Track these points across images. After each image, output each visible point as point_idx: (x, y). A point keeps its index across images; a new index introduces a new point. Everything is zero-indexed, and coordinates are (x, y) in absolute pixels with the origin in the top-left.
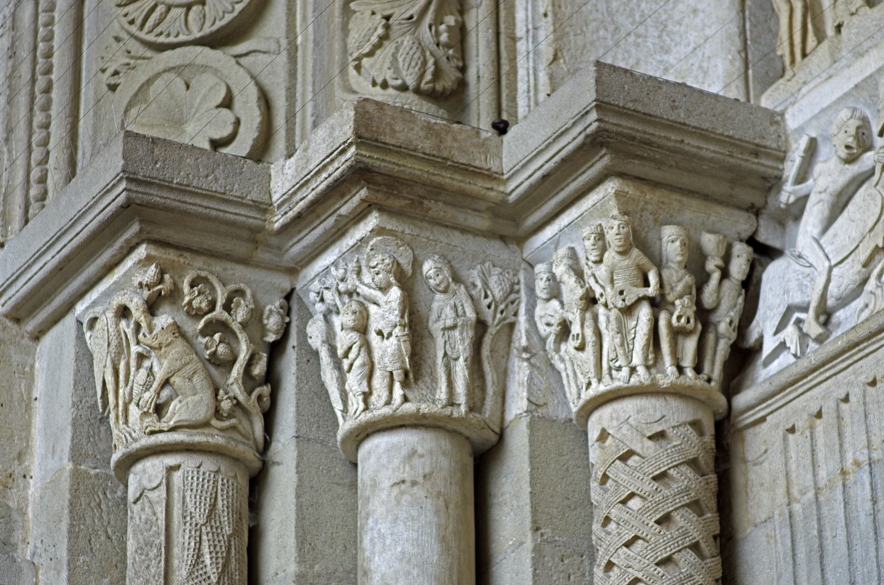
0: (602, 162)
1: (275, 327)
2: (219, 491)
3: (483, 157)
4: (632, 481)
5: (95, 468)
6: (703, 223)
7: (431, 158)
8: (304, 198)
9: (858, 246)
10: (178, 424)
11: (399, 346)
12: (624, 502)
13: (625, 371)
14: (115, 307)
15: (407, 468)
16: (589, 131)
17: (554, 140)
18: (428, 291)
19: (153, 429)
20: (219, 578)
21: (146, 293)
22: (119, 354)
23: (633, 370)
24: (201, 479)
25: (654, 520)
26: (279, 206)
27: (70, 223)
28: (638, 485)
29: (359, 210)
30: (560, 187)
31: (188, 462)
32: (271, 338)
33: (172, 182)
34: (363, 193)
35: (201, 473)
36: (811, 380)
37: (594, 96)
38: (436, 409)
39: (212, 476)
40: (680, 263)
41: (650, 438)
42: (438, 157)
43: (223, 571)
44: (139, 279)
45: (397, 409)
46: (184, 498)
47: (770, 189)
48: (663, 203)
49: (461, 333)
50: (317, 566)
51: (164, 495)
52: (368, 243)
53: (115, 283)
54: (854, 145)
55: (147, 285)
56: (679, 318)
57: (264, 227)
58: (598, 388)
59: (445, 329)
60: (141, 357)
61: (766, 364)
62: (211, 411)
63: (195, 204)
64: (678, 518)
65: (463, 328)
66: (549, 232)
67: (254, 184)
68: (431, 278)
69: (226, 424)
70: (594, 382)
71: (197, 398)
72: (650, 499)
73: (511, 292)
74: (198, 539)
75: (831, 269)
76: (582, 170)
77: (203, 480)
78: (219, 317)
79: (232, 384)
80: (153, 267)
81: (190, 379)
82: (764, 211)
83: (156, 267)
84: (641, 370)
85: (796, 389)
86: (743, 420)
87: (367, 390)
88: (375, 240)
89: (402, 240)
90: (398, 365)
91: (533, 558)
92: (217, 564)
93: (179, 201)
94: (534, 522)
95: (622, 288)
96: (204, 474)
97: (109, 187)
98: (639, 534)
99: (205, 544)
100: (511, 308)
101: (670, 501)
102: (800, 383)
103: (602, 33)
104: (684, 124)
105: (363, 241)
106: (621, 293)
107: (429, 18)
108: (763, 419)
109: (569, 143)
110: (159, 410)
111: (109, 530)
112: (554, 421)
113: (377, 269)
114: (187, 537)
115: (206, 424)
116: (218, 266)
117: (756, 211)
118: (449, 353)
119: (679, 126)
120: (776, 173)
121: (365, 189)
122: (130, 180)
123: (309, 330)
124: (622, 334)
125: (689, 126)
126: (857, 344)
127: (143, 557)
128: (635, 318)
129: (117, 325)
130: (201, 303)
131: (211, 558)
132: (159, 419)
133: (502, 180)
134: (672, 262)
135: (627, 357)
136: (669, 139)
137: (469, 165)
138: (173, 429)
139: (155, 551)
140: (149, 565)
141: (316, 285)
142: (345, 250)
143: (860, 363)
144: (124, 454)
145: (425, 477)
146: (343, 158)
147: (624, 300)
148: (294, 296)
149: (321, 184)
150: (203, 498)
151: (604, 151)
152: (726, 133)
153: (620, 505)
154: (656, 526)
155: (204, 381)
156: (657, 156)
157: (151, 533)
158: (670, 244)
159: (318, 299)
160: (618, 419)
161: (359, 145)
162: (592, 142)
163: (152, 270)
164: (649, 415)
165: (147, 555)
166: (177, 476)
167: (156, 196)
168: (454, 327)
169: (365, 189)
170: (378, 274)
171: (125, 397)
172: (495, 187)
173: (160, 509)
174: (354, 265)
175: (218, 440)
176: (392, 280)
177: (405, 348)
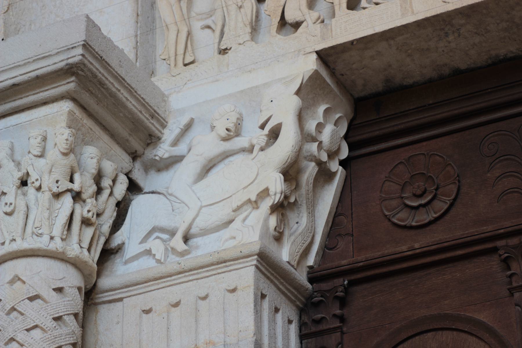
6: (106, 153)
9: (231, 196)
12: (28, 330)
13: (46, 238)
16: (71, 61)
23: (52, 238)
30: (20, 97)
36: (174, 280)
37: (84, 38)
40: (93, 174)
41: (54, 290)
47: (148, 145)
48: (91, 129)
54: (233, 129)
56: (89, 211)
58: (20, 245)
61: (126, 263)
72: (49, 332)
75: (201, 207)
76: (47, 88)
82: (139, 159)
84: (58, 240)
85: (158, 284)
101: (63, 338)
104: (124, 79)
106: (57, 182)
108: (121, 300)
109: (49, 66)
117: (134, 156)
119: (121, 79)
120: (159, 134)
124: (50, 211)
125: (126, 82)
126: (225, 262)
134: (88, 172)
135: (50, 228)
143: (223, 275)
147: (58, 187)
151: (73, 78)
152: (142, 96)
153: (26, 332)
156: (99, 96)
158: (89, 159)
162: (68, 69)
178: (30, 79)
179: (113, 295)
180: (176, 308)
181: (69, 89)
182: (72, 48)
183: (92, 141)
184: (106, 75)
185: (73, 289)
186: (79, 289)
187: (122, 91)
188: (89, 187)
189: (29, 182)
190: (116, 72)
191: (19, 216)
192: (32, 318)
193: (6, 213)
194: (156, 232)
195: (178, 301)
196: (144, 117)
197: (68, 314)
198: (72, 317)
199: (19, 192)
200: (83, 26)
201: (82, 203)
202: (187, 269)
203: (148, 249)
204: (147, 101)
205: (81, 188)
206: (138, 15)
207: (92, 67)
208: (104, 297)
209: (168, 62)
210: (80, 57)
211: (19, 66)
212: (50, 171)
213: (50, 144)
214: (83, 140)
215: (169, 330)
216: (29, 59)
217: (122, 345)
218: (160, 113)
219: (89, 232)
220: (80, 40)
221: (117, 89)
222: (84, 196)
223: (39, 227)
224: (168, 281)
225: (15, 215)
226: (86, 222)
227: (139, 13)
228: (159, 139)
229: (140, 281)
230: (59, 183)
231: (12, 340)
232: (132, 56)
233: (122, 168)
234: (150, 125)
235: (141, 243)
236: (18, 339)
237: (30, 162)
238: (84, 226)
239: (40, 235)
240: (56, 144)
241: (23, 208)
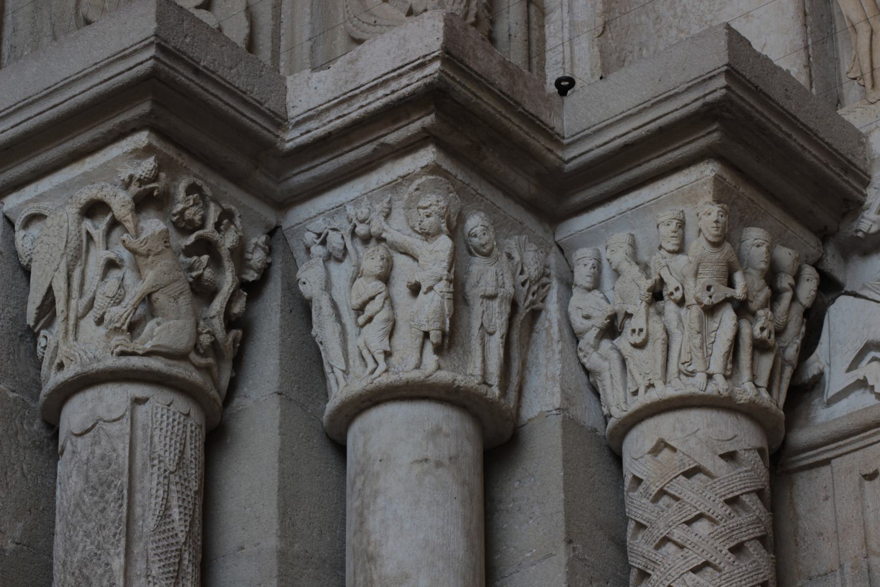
0: (711, 137)
1: (259, 265)
2: (188, 438)
3: (548, 114)
4: (702, 501)
5: (13, 391)
7: (505, 98)
8: (344, 115)
10: (155, 349)
11: (442, 303)
12: (689, 523)
13: (701, 378)
14: (83, 201)
15: (431, 446)
16: (709, 98)
17: (653, 105)
18: (465, 252)
19: (124, 349)
20: (186, 538)
21: (135, 189)
22: (76, 258)
23: (710, 377)
24: (171, 420)
25: (727, 547)
26: (298, 124)
27: (44, 93)
28: (709, 506)
29: (412, 141)
30: (637, 163)
31: (158, 397)
32: (251, 276)
33: (198, 63)
34: (428, 120)
35: (171, 414)
37: (726, 60)
38: (473, 382)
39: (182, 419)
40: (762, 270)
41: (722, 456)
42: (511, 99)
43: (190, 531)
44: (130, 172)
45: (431, 375)
46: (152, 437)
47: (844, 215)
48: (752, 201)
49: (500, 306)
50: (296, 546)
51: (128, 430)
52: (412, 181)
53: (85, 174)
55: (139, 180)
57: (275, 144)
58: (662, 392)
59: (484, 297)
60: (111, 265)
61: (830, 403)
62: (192, 344)
63: (216, 96)
64: (751, 550)
65: (502, 300)
66: (599, 214)
67: (272, 92)
68: (475, 236)
69: (203, 361)
70: (659, 384)
71: (180, 323)
72: (722, 523)
74: (166, 487)
76: (677, 145)
77: (174, 420)
78: (210, 235)
79: (214, 317)
80: (152, 160)
81: (176, 299)
83: (155, 161)
84: (719, 379)
86: (799, 460)
87: (388, 349)
88: (424, 178)
89: (453, 185)
90: (438, 325)
91: (567, 573)
92: (186, 521)
93: (202, 87)
94: (568, 533)
95: (710, 283)
96: (174, 414)
97: (127, 52)
98: (711, 560)
99: (174, 496)
101: (744, 529)
103: (643, 18)
104: (795, 118)
105: (407, 178)
106: (709, 288)
108: (827, 462)
109: (677, 110)
110: (133, 328)
111: (25, 467)
112: (582, 426)
113: (429, 211)
114: (155, 483)
115: (180, 356)
116: (213, 179)
117: (824, 236)
118: (486, 325)
120: (860, 197)
121: (433, 116)
122: (161, 48)
123: (301, 275)
124: (702, 335)
125: (798, 121)
127: (96, 498)
128: (717, 320)
129: (79, 223)
130: (194, 215)
131: (180, 513)
132: (132, 338)
133: (562, 144)
134: (754, 269)
135: (705, 362)
136: (781, 129)
137: (537, 117)
138: (148, 354)
139: (115, 492)
140: (105, 509)
141: (320, 225)
142: (375, 187)
144: (77, 374)
145: (450, 459)
146: (418, 75)
148: (278, 234)
149: (377, 100)
150: (173, 442)
152: (827, 140)
153: (686, 526)
154: (730, 554)
155: (189, 306)
157: (109, 471)
158: (754, 248)
159: (318, 241)
160: (682, 430)
161: (445, 61)
163: (148, 165)
164: (720, 431)
165: (102, 496)
166: (141, 409)
167: (184, 76)
168: (492, 297)
169: (433, 116)
170: (428, 216)
171: (77, 311)
172: (555, 151)
173: (121, 445)
174: (385, 205)
175: (196, 377)
176: (444, 226)
177: (447, 307)
179: (814, 456)
182: (710, 78)
183: (755, 219)
184: (766, 113)
185: (751, 452)
186: (761, 451)
187: (794, 136)
188: (759, 291)
189: (665, 293)
190: (782, 108)
191: (656, 349)
192: (693, 503)
193: (635, 346)
194: (870, 350)
197: (748, 493)
198: (755, 497)
200: (723, 42)
201: (751, 318)
203: (862, 378)
204: (835, 146)
205: (747, 293)
206: (805, 14)
207: (743, 104)
209: (861, 82)
210: (724, 91)
211: (631, 115)
212: (696, 274)
213: (691, 231)
214: (741, 220)
217: (836, 532)
218: (858, 163)
219: (766, 362)
220: (720, 65)
221: (786, 134)
222: (753, 306)
225: (649, 346)
226: (760, 347)
227: (807, 10)
228: (860, 204)
229: (854, 430)
230: (712, 290)
231: (666, 540)
232: (803, 80)
233: (807, 257)
234: (844, 184)
235: (849, 370)
236: (675, 538)
237: (663, 262)
238: (757, 354)
239: (691, 374)
240: (700, 231)
241: (660, 335)
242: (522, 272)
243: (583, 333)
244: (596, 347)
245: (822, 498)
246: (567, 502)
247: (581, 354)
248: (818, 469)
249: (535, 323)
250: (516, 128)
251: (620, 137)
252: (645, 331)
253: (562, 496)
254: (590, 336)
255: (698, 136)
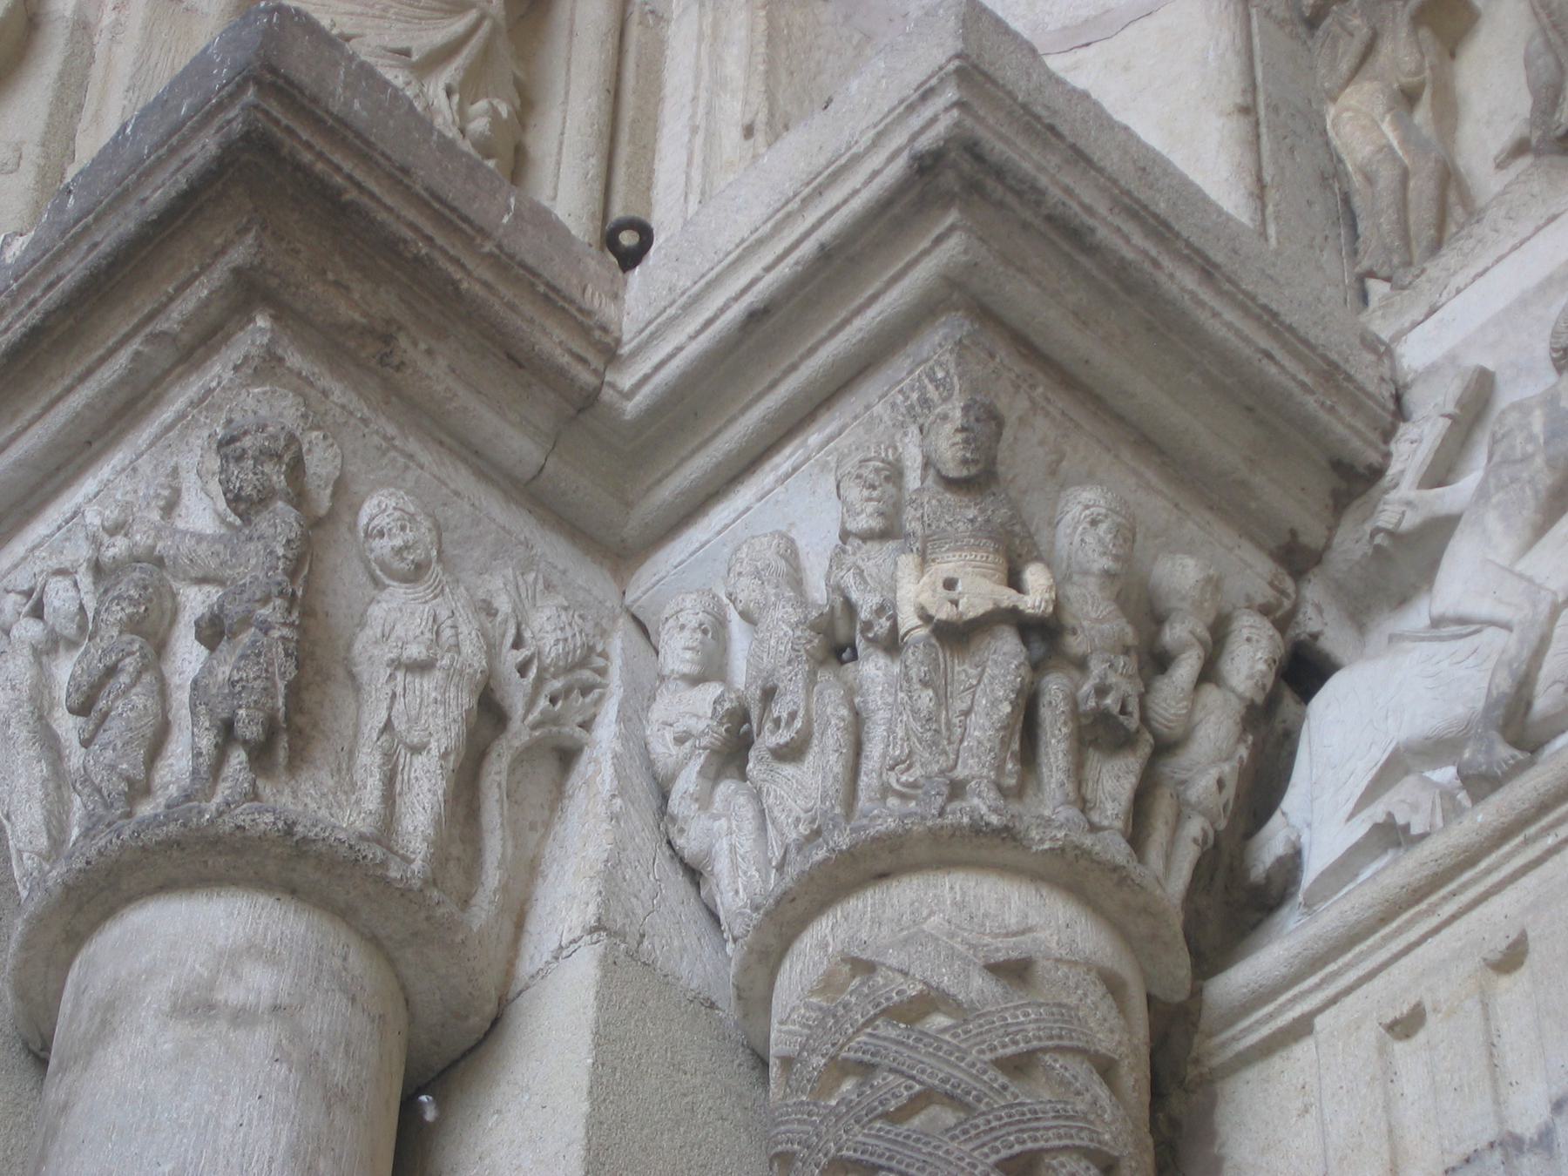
16: (925, 143)
18: (363, 578)
37: (953, 45)
59: (396, 664)
68: (381, 534)
73: (583, 663)
76: (870, 292)
86: (1234, 1039)
100: (577, 701)
102: (1452, 886)
107: (450, 73)
136: (1127, 240)
147: (955, 603)
151: (952, 216)
159: (26, 609)
168: (422, 667)
178: (800, 268)
179: (1271, 1016)
180: (1517, 975)
181: (947, 264)
186: (1113, 985)
195: (1514, 936)
196: (1286, 372)
199: (824, 675)
202: (1527, 806)
205: (1058, 604)
208: (1239, 1039)
215: (1495, 1052)
216: (787, 203)
220: (942, 59)
222: (1075, 644)
223: (904, 762)
224: (1464, 887)
227: (1267, 178)
229: (1359, 922)
238: (1093, 757)
241: (834, 712)
242: (518, 643)
243: (673, 778)
244: (704, 801)
245: (1295, 1113)
246: (594, 1123)
247: (673, 831)
248: (1284, 1054)
249: (567, 780)
250: (477, 288)
251: (736, 299)
252: (801, 713)
253: (585, 1107)
254: (687, 782)
255: (914, 253)
